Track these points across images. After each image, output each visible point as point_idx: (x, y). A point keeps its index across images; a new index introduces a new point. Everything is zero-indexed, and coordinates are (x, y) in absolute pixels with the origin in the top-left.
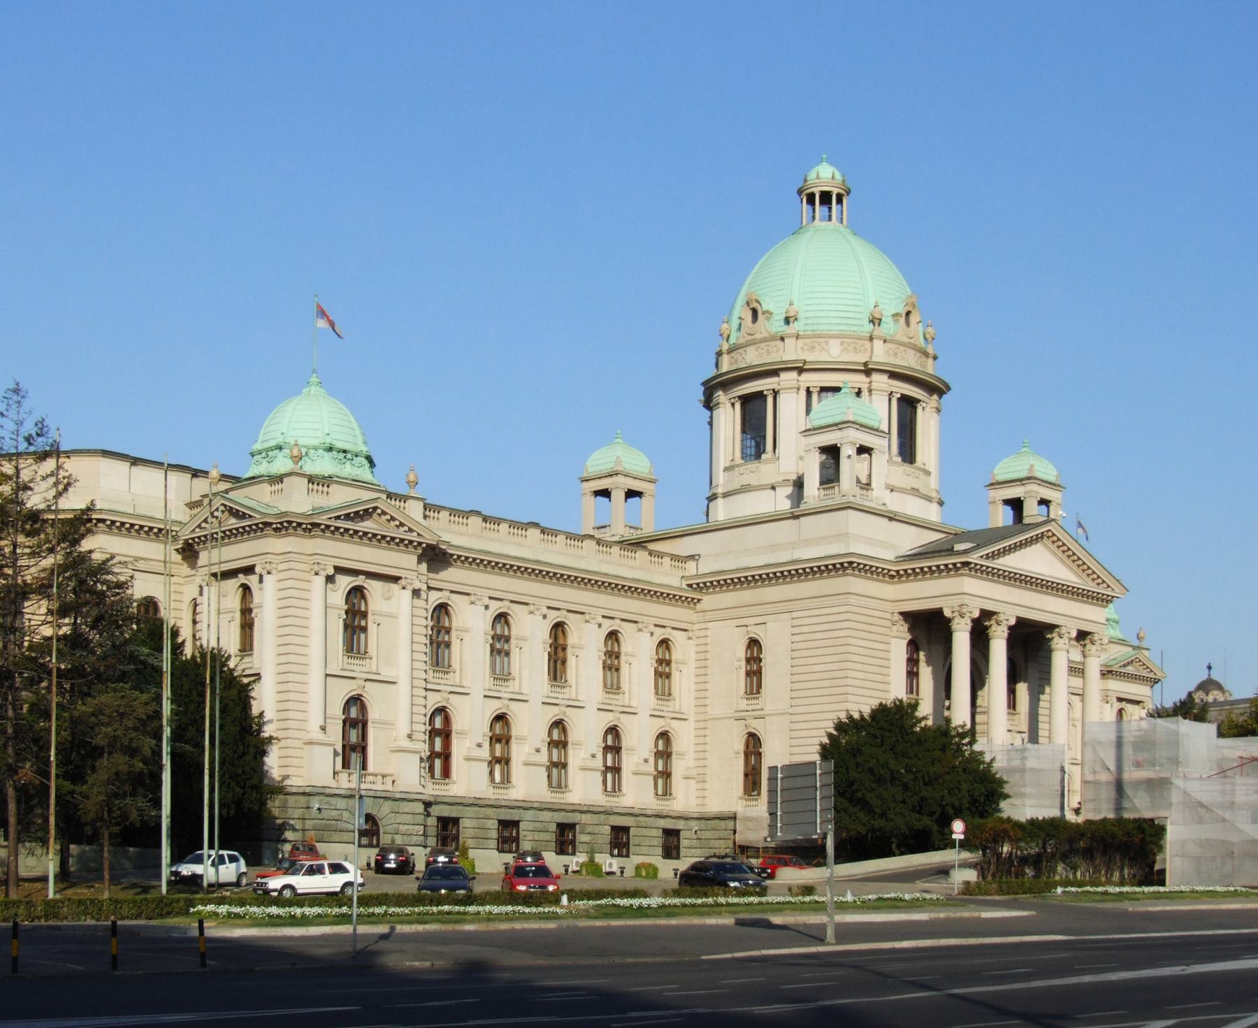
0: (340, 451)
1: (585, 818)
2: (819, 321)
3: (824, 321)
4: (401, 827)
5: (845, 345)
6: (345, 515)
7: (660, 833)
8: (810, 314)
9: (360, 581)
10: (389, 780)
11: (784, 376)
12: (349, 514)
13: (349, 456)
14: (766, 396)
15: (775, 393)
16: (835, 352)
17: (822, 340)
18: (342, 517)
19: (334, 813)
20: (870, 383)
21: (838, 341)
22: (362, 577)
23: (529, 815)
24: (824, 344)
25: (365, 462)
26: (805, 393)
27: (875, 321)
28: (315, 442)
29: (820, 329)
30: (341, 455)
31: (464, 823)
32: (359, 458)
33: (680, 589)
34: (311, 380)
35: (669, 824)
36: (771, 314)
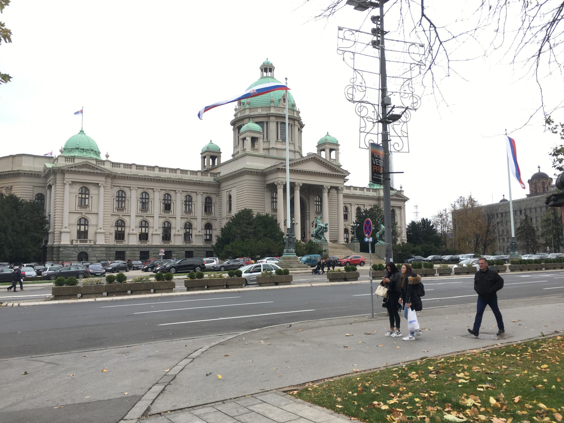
0: (81, 149)
1: (174, 249)
2: (256, 103)
5: (263, 110)
6: (75, 167)
7: (205, 252)
8: (253, 102)
9: (85, 185)
10: (92, 242)
11: (245, 120)
13: (85, 150)
16: (259, 112)
19: (69, 252)
21: (261, 109)
22: (85, 184)
23: (153, 249)
24: (257, 110)
30: (82, 150)
31: (127, 252)
33: (213, 183)
36: (244, 103)
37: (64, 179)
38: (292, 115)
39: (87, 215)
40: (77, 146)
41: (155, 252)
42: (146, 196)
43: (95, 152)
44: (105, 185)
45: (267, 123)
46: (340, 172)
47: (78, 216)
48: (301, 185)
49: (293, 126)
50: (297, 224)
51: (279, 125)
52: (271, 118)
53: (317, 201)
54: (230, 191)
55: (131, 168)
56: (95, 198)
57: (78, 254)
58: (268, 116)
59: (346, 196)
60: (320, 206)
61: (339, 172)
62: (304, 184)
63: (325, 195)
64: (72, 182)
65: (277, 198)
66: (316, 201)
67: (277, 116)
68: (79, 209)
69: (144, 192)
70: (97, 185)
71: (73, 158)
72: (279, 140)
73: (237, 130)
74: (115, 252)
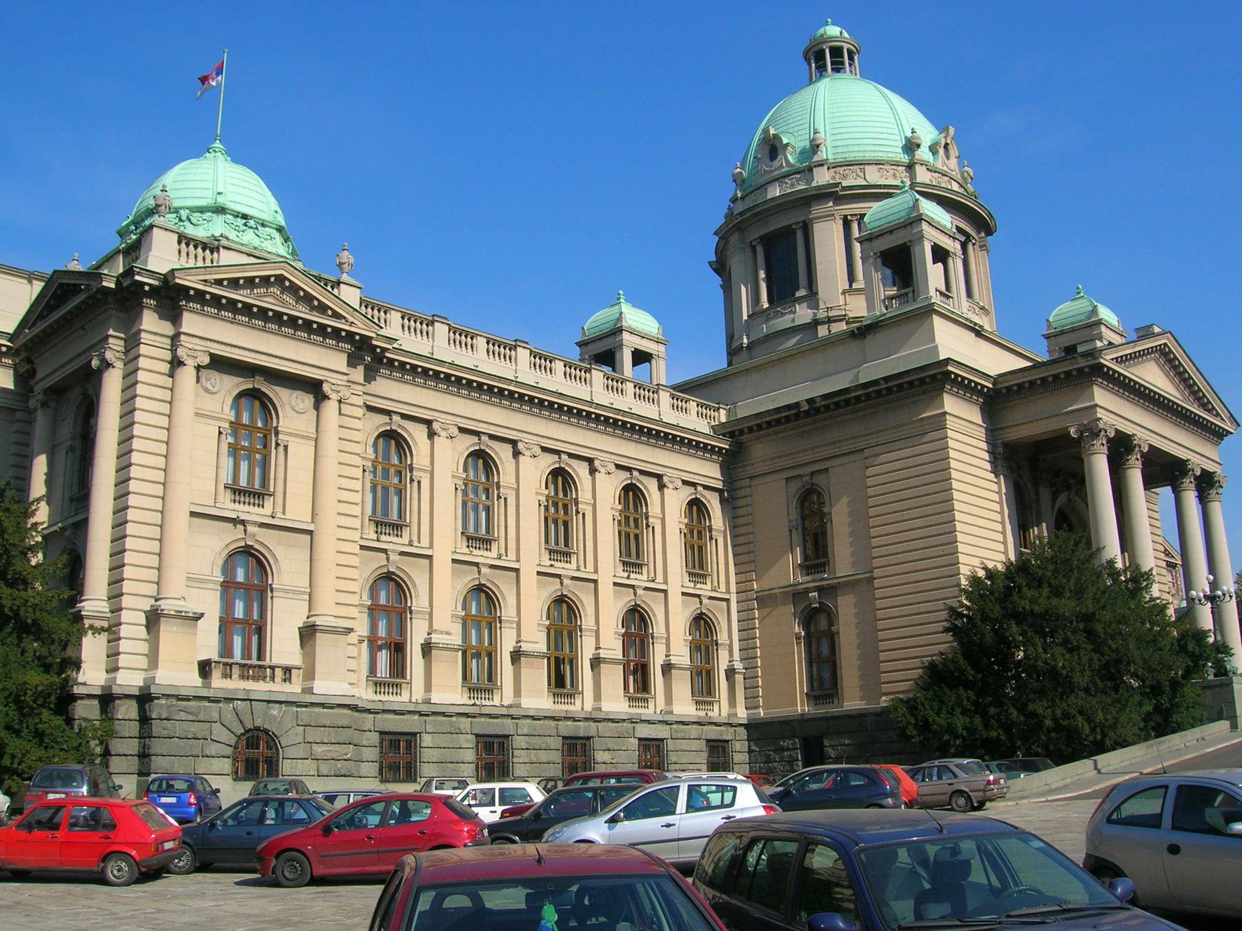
0: (237, 215)
3: (856, 148)
4: (315, 747)
12: (237, 279)
13: (252, 223)
14: (794, 232)
15: (807, 228)
17: (855, 167)
18: (225, 283)
19: (193, 729)
25: (276, 235)
26: (841, 222)
28: (202, 203)
29: (851, 157)
30: (240, 222)
31: (427, 740)
32: (267, 229)
35: (713, 733)
37: (175, 339)
39: (267, 536)
40: (221, 200)
41: (536, 741)
44: (345, 393)
47: (229, 537)
54: (812, 473)
56: (300, 454)
57: (233, 740)
64: (211, 355)
68: (229, 507)
70: (314, 388)
71: (211, 246)
73: (760, 250)
74: (375, 737)
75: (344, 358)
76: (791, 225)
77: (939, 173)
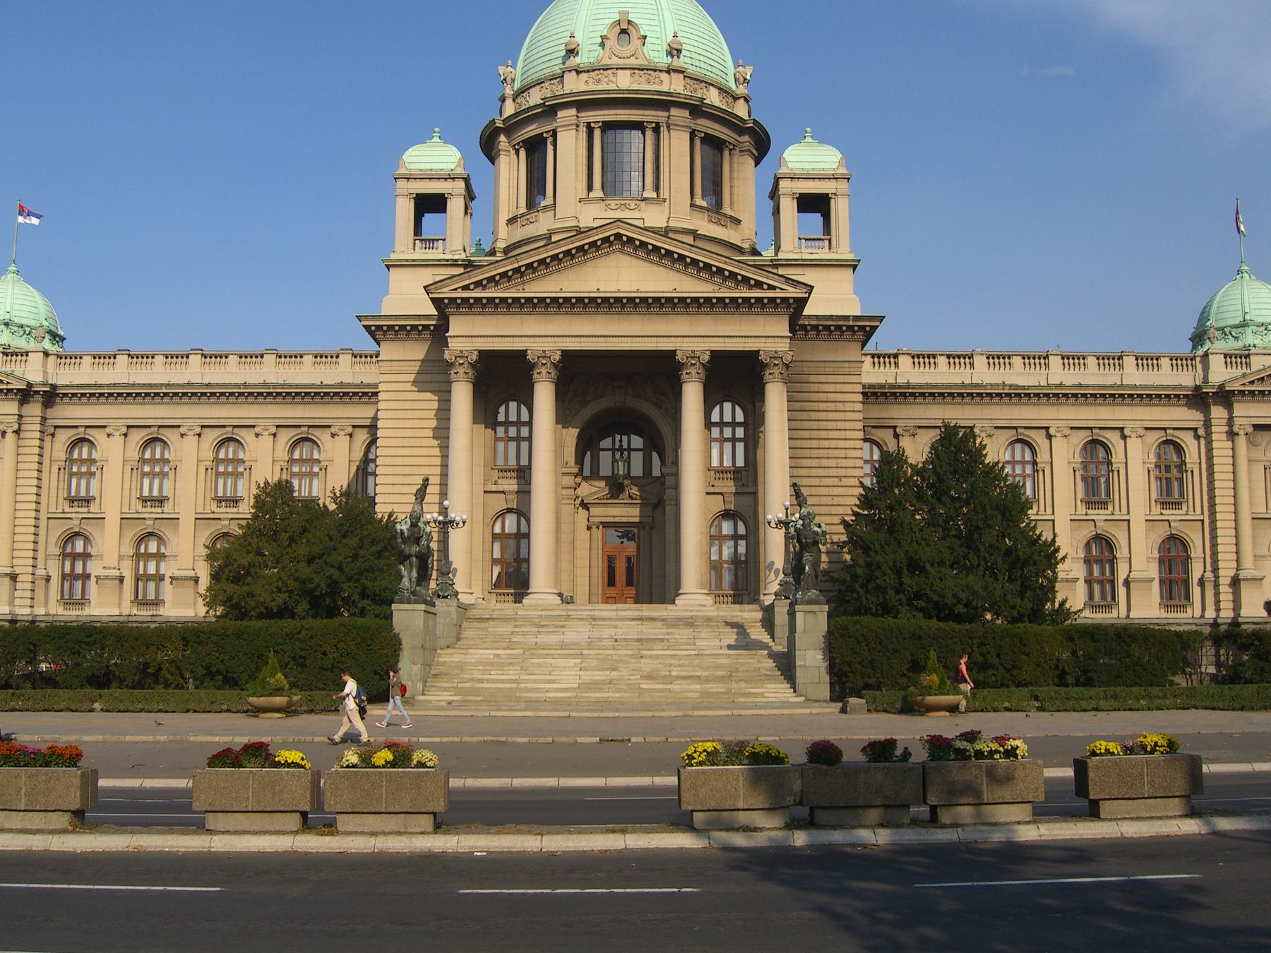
16: (535, 98)
20: (669, 117)
27: (571, 52)
34: (10, 268)
38: (664, 88)
42: (162, 453)
43: (22, 326)
45: (554, 134)
46: (759, 285)
48: (474, 357)
49: (663, 130)
50: (464, 523)
51: (597, 133)
52: (560, 114)
53: (728, 424)
55: (896, 364)
58: (549, 110)
59: (873, 395)
60: (740, 447)
61: (751, 287)
62: (569, 357)
63: (692, 395)
65: (530, 424)
66: (733, 424)
67: (583, 104)
69: (1018, 441)
72: (592, 195)
75: (16, 404)
76: (644, 122)
77: (599, 70)
